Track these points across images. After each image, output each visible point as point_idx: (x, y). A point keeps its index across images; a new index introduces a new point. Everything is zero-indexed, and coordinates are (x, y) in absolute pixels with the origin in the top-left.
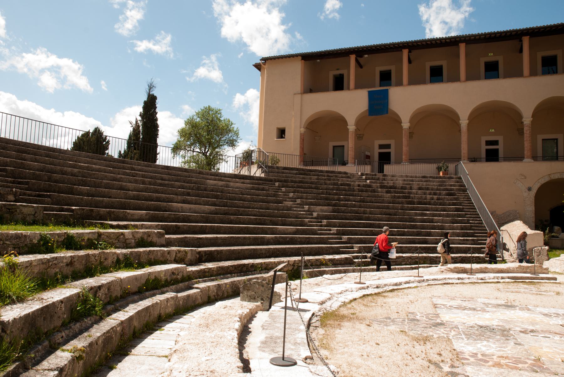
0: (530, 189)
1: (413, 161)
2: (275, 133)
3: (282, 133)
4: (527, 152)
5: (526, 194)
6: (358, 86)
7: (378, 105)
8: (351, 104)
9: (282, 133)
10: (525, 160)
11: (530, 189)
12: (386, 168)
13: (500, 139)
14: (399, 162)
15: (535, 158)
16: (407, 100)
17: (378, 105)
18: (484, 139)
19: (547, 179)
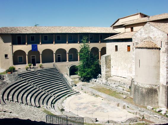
0: (68, 68)
3: (6, 56)
6: (28, 44)
8: (26, 48)
13: (61, 55)
15: (69, 61)
16: (41, 47)
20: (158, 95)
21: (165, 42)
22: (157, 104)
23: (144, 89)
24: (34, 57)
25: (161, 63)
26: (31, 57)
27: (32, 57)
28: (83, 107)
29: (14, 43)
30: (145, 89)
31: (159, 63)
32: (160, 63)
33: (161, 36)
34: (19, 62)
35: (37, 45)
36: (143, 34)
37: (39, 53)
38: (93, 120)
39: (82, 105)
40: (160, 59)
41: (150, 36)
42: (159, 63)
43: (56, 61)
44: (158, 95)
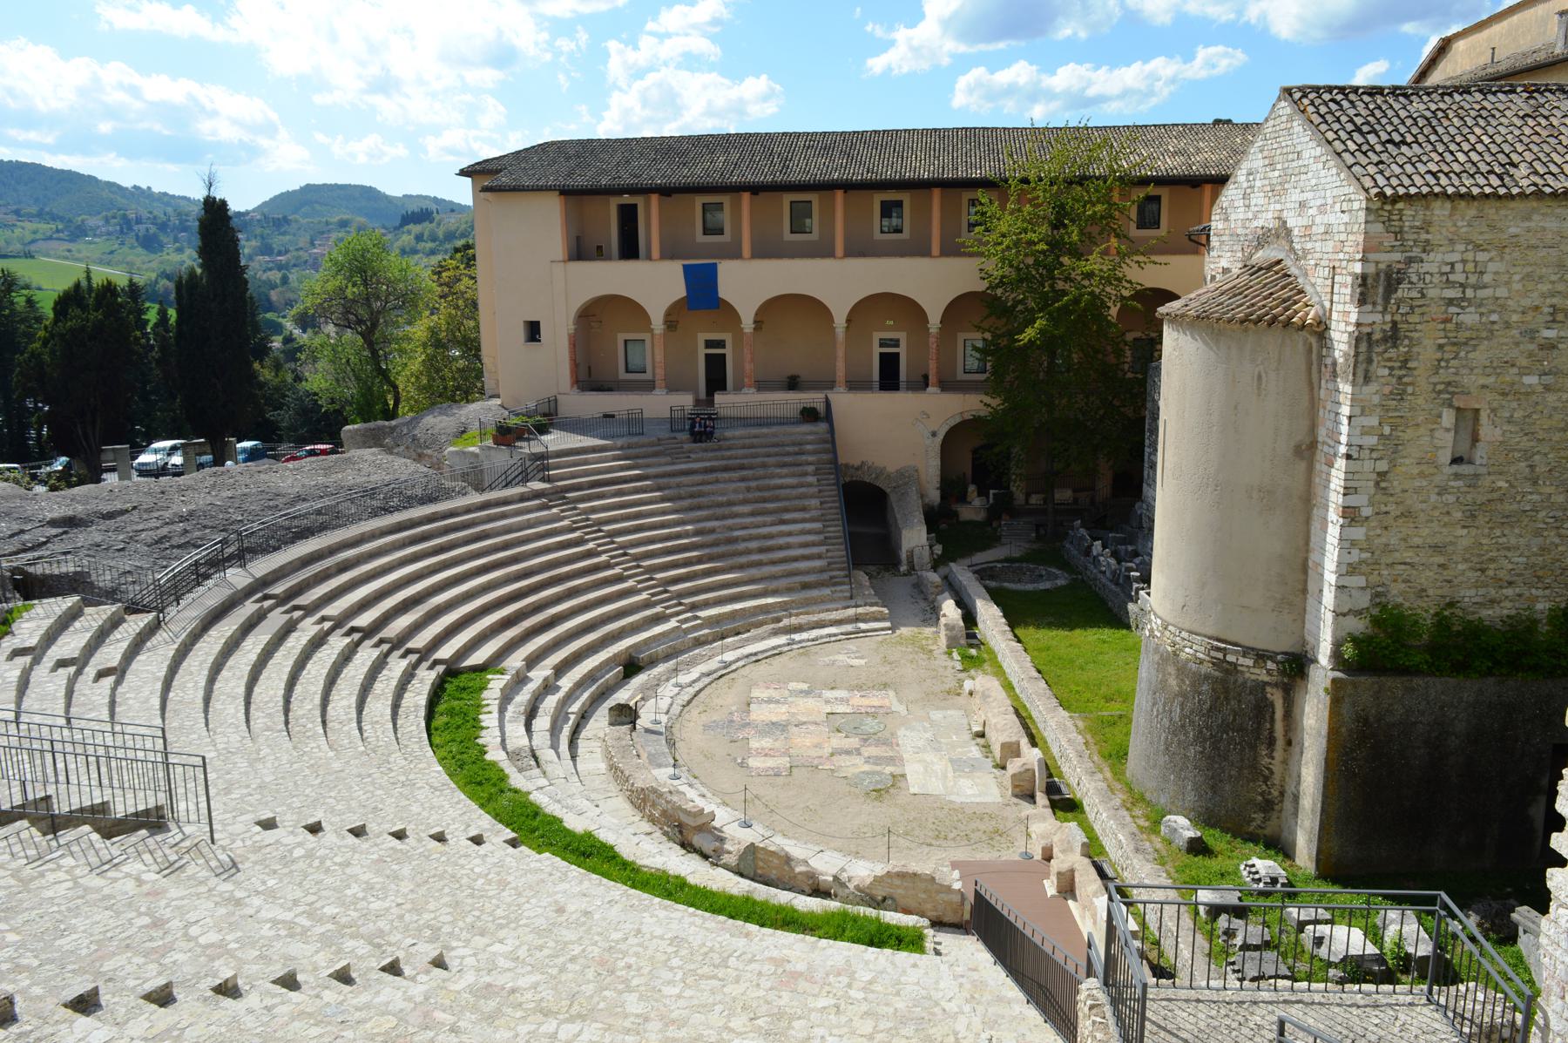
0: (934, 434)
1: (762, 385)
2: (521, 333)
3: (533, 331)
4: (932, 379)
5: (928, 442)
6: (668, 254)
7: (702, 291)
8: (655, 284)
9: (533, 331)
10: (930, 389)
11: (934, 434)
12: (719, 398)
14: (738, 388)
17: (702, 291)
18: (877, 336)
19: (958, 420)
20: (1271, 742)
21: (1349, 279)
22: (1259, 816)
23: (1171, 669)
24: (720, 344)
25: (1318, 466)
26: (701, 345)
27: (709, 344)
28: (774, 719)
29: (581, 250)
30: (1182, 670)
31: (1303, 465)
32: (1310, 469)
33: (1336, 219)
34: (623, 375)
35: (713, 269)
36: (1258, 199)
37: (727, 312)
38: (684, 818)
39: (784, 709)
40: (1313, 428)
41: (1285, 214)
42: (1303, 465)
43: (856, 384)
44: (1296, 749)
